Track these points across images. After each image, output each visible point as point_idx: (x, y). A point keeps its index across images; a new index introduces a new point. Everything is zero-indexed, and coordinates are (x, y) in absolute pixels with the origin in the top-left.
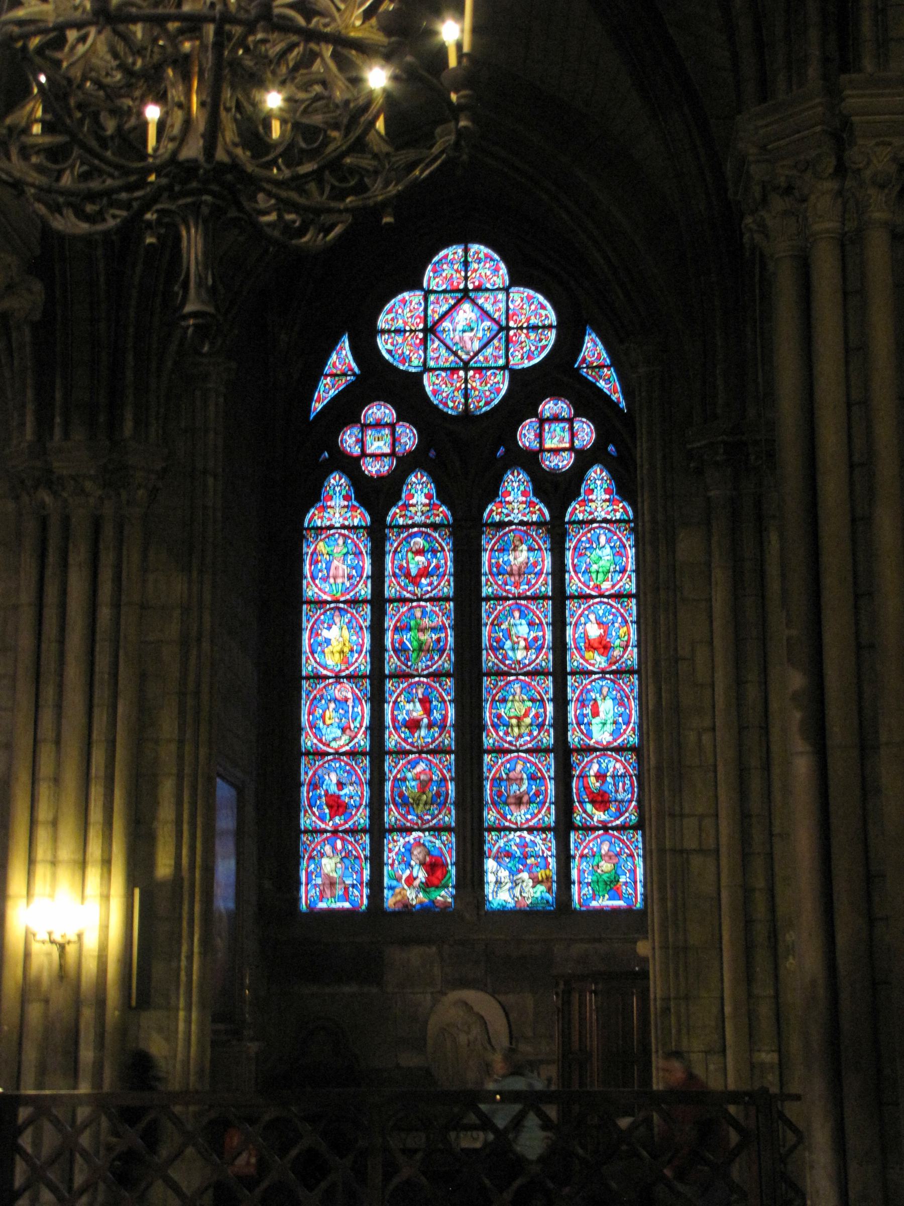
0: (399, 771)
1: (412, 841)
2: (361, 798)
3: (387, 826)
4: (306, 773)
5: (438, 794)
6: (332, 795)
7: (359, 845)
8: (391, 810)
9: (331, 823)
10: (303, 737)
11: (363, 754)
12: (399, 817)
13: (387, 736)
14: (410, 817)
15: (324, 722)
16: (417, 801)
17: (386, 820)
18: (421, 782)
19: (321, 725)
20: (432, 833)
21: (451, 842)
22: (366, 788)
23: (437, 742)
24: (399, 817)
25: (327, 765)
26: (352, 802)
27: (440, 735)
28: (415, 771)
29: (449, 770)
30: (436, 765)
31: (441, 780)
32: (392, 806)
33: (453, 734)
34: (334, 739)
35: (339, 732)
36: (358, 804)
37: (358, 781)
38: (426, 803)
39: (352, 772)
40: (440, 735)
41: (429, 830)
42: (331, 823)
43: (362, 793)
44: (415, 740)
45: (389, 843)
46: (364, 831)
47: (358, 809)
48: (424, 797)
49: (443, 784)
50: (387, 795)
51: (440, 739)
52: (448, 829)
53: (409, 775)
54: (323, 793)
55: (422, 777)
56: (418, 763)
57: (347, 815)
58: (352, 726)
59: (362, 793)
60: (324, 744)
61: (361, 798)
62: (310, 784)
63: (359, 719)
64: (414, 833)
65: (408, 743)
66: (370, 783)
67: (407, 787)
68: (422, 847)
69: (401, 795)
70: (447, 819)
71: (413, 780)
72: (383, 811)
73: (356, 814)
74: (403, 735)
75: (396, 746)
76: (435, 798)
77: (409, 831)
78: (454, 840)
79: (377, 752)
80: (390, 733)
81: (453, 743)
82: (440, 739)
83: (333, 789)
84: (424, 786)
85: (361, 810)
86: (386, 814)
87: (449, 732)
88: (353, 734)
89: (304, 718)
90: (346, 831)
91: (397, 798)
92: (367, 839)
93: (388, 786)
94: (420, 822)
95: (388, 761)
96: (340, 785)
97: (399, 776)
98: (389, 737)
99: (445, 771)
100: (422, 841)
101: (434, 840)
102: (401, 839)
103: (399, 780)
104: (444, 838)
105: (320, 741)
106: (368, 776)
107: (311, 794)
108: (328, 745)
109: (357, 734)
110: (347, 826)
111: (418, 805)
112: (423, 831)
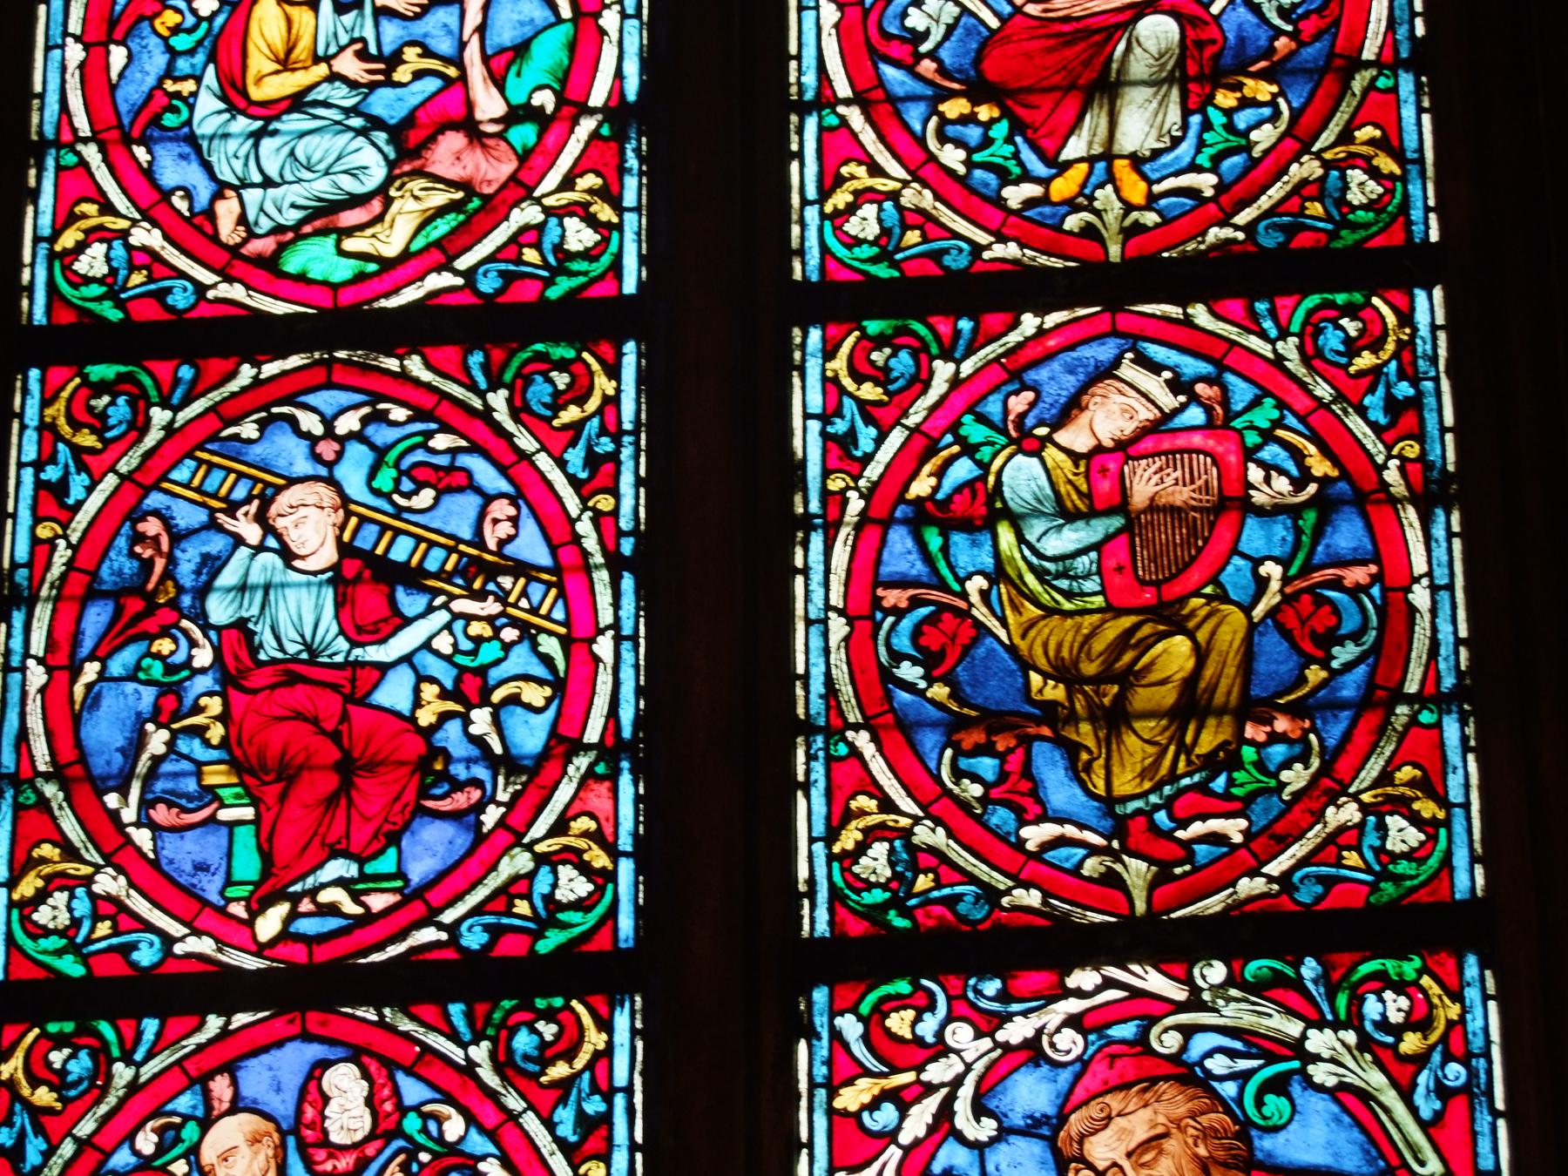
0: (922, 447)
1: (1070, 1043)
2: (569, 691)
3: (817, 921)
4: (54, 501)
5: (1306, 622)
6: (291, 672)
7: (547, 1100)
8: (849, 778)
9: (269, 925)
10: (40, 216)
11: (594, 319)
12: (928, 835)
13: (804, 175)
14: (1034, 835)
15: (235, 97)
16: (1104, 697)
17: (809, 861)
18: (1135, 523)
19: (208, 111)
20: (1255, 968)
21: (1455, 1044)
22: (614, 602)
23: (1276, 192)
24: (928, 835)
25: (249, 430)
26: (481, 720)
27: (1298, 140)
28: (1076, 437)
29: (1403, 418)
30: (1270, 378)
31: (1326, 506)
32: (862, 740)
33: (1418, 129)
34: (324, 217)
35: (370, 162)
36: (530, 735)
37: (532, 547)
38: (1192, 704)
39: (486, 474)
40: (1298, 140)
41: (1233, 936)
42: (269, 925)
43: (577, 640)
44: (1063, 187)
45: (842, 1071)
46: (592, 972)
47: (536, 775)
48: (1175, 654)
49: (1348, 534)
50: (819, 654)
51: (1308, 168)
52: (1420, 924)
53: (1023, 478)
54: (203, 657)
55: (1145, 482)
56: (1106, 372)
57: (429, 849)
58: (488, 105)
59: (577, 640)
60: (230, 262)
61: (569, 691)
62: (82, 586)
63: (550, 51)
64: (1084, 978)
65: (1004, 223)
66: (653, 562)
67: (998, 574)
68: (1173, 1102)
69: (948, 640)
70: (1402, 834)
71: (1068, 516)
72: (788, 787)
73: (513, 833)
74: (952, 157)
75: (886, 245)
76: (1274, 654)
77: (1036, 953)
78: (1487, 1022)
79: (718, 305)
80: (838, 147)
81: (1423, 193)
82: (1308, 168)
83: (302, 616)
84: (1161, 562)
85: (564, 793)
86: (809, 812)
87: (1380, 107)
88: (495, 170)
89: (56, 74)
90: (421, 983)
91: (909, 672)
92: (621, 1038)
93: (822, 574)
94: (1137, 872)
95: (816, 367)
96: (368, 584)
97: (921, 487)
98: (830, 182)
99: (1355, 423)
100: (1170, 1042)
101: (1294, 1028)
102: (960, 1034)
103: (924, 514)
104: (1396, 1007)
105: (195, 232)
106: (630, 503)
107: (91, 670)
108: (266, 270)
109: (531, 163)
110: (428, 935)
111: (1115, 720)
112: (1175, 946)
